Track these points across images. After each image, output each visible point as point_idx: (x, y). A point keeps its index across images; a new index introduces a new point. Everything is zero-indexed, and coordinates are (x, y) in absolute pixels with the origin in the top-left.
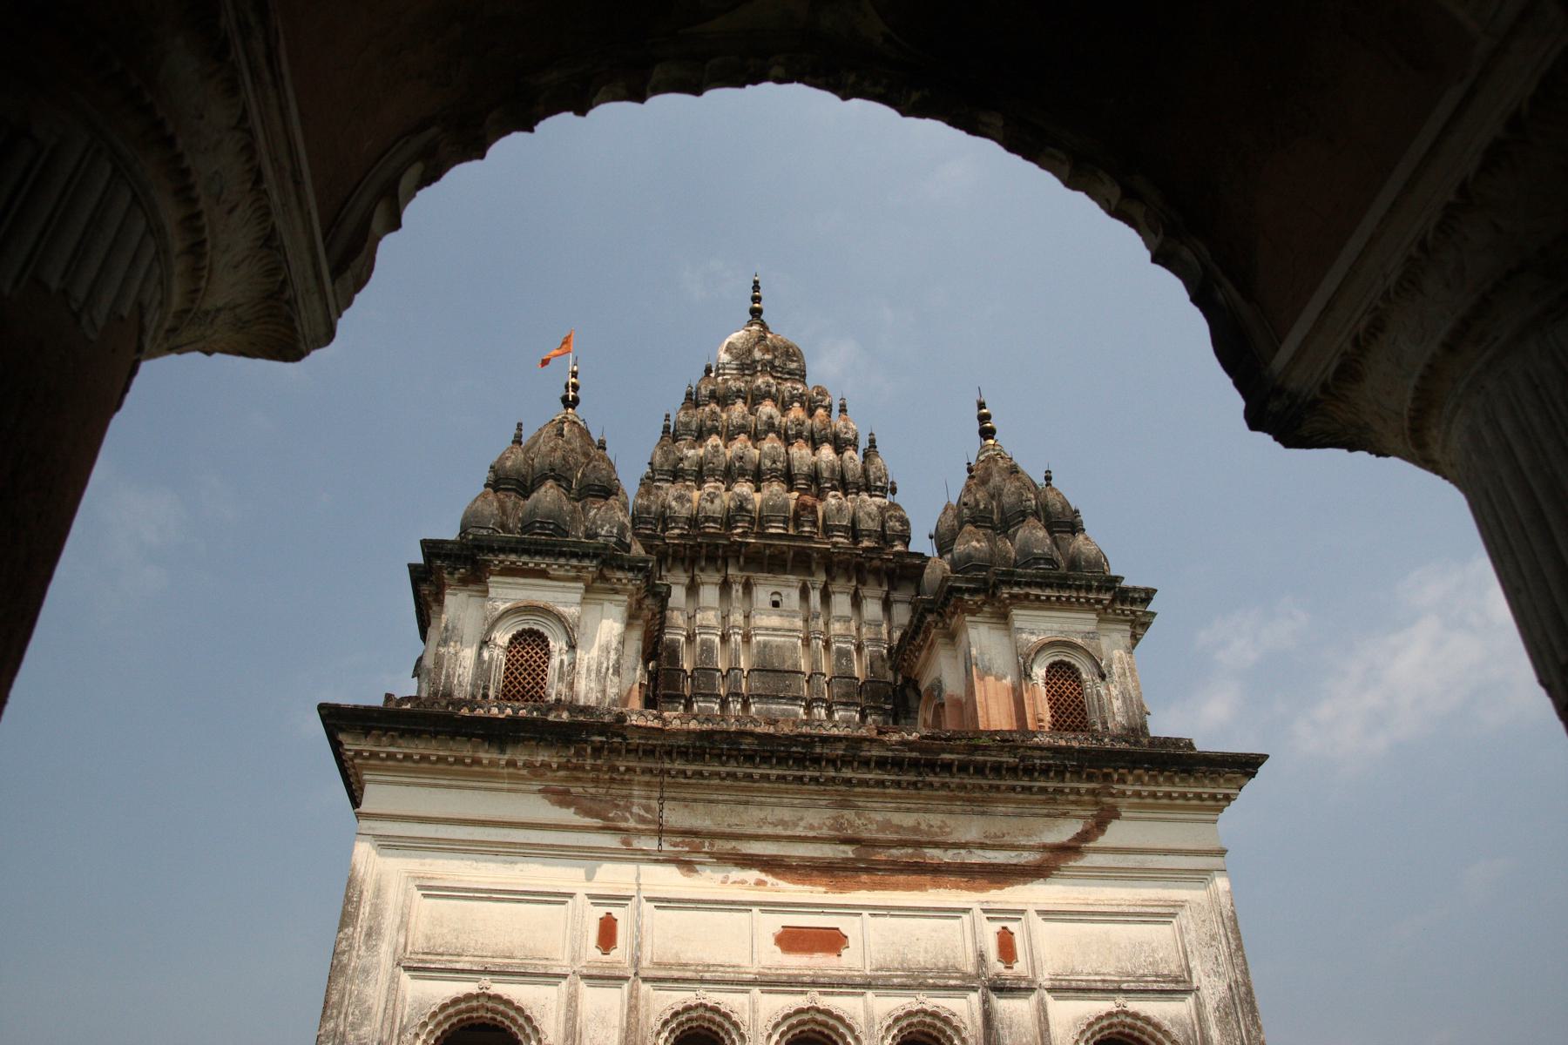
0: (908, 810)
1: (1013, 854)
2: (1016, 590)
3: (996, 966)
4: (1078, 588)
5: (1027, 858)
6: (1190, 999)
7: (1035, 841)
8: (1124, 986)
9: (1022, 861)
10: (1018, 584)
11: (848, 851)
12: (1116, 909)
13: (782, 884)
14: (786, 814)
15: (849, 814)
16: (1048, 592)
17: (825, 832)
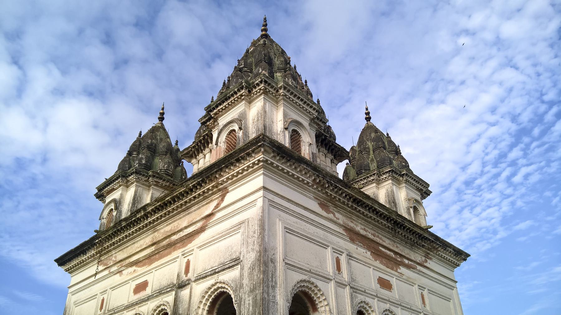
0: (170, 224)
1: (194, 226)
2: (215, 111)
3: (184, 278)
4: (232, 95)
5: (199, 225)
6: (239, 266)
7: (203, 216)
8: (217, 271)
9: (196, 228)
10: (214, 109)
11: (153, 248)
12: (221, 235)
13: (139, 269)
14: (141, 242)
15: (156, 234)
16: (225, 104)
17: (150, 243)
